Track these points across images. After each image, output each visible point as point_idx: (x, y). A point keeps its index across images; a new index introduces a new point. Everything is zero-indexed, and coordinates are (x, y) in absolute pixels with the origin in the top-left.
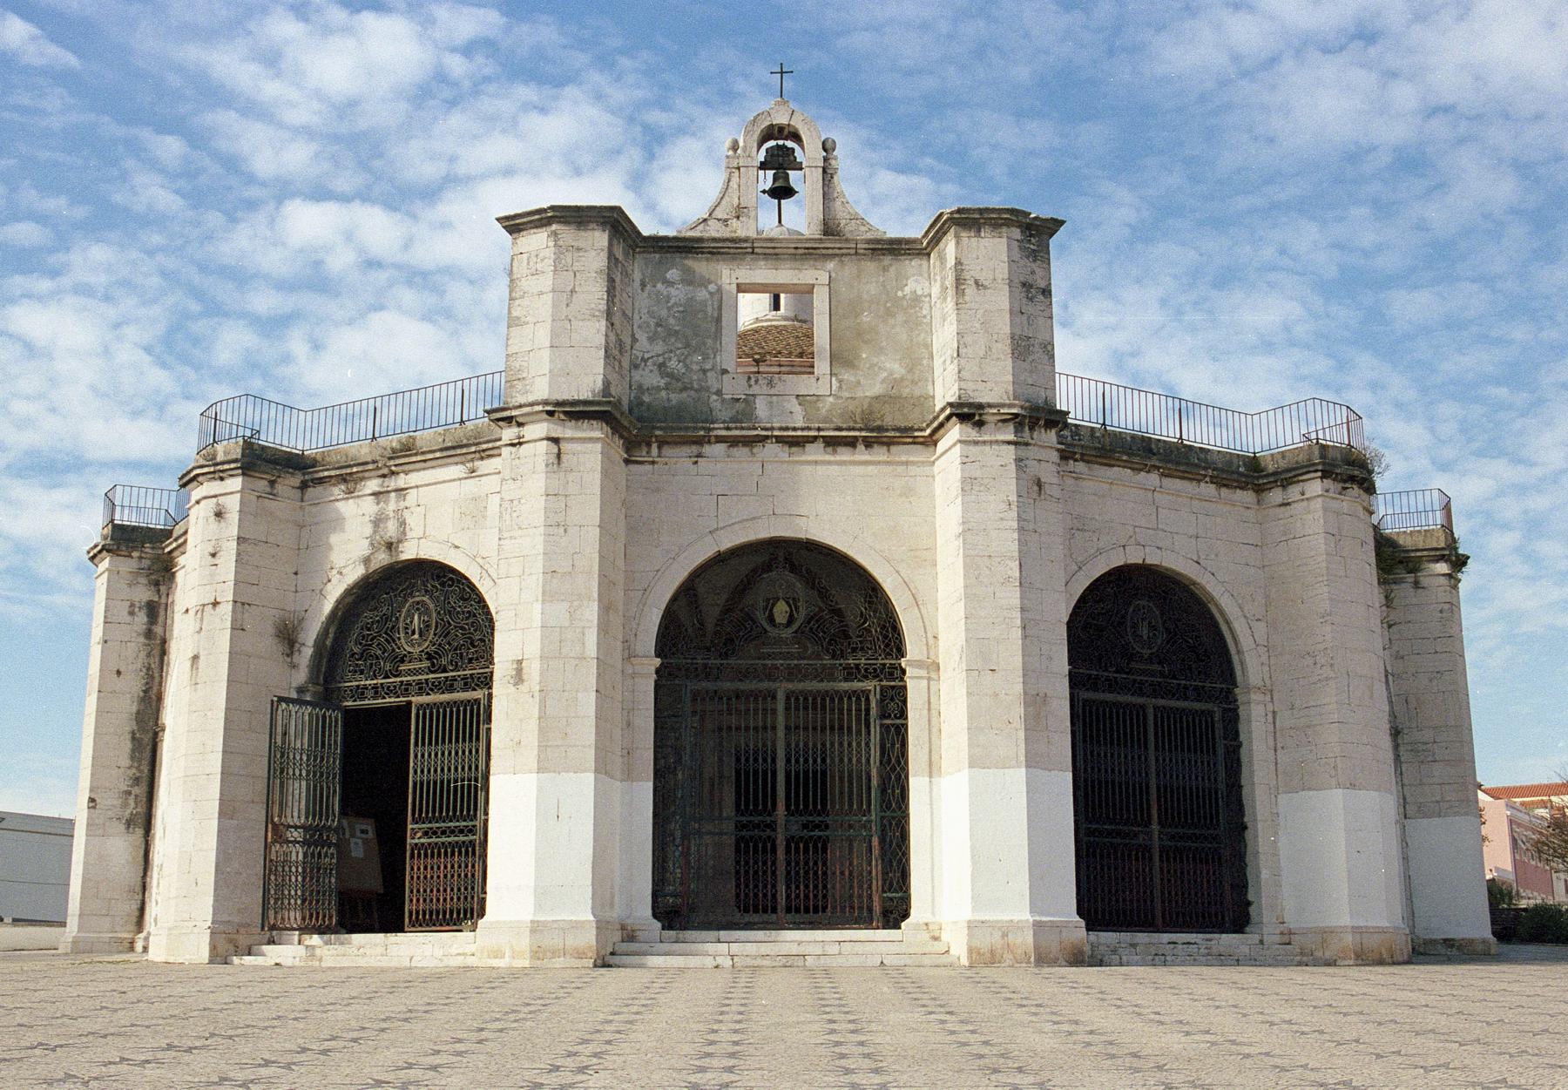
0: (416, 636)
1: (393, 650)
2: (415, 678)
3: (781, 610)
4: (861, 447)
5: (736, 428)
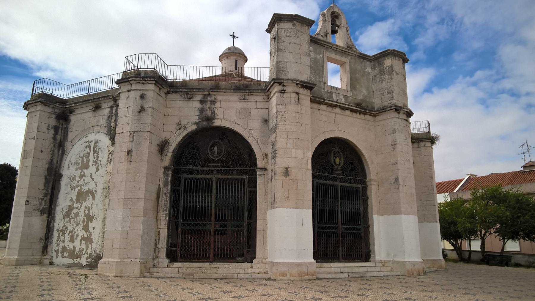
1: (206, 158)
2: (215, 168)
3: (337, 160)
4: (358, 114)
5: (332, 101)
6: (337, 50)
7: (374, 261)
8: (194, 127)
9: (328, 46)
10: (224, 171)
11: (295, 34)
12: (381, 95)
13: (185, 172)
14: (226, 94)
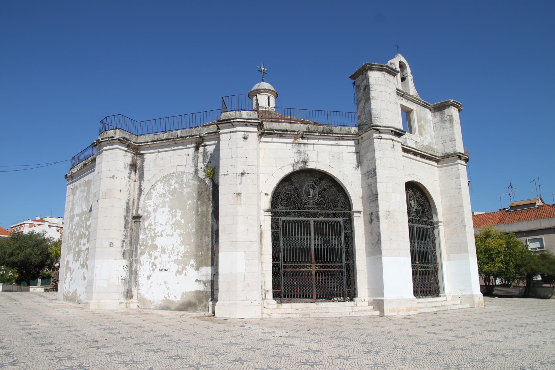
0: (311, 196)
1: (301, 200)
7: (445, 296)
10: (320, 213)
12: (443, 142)
13: (282, 214)
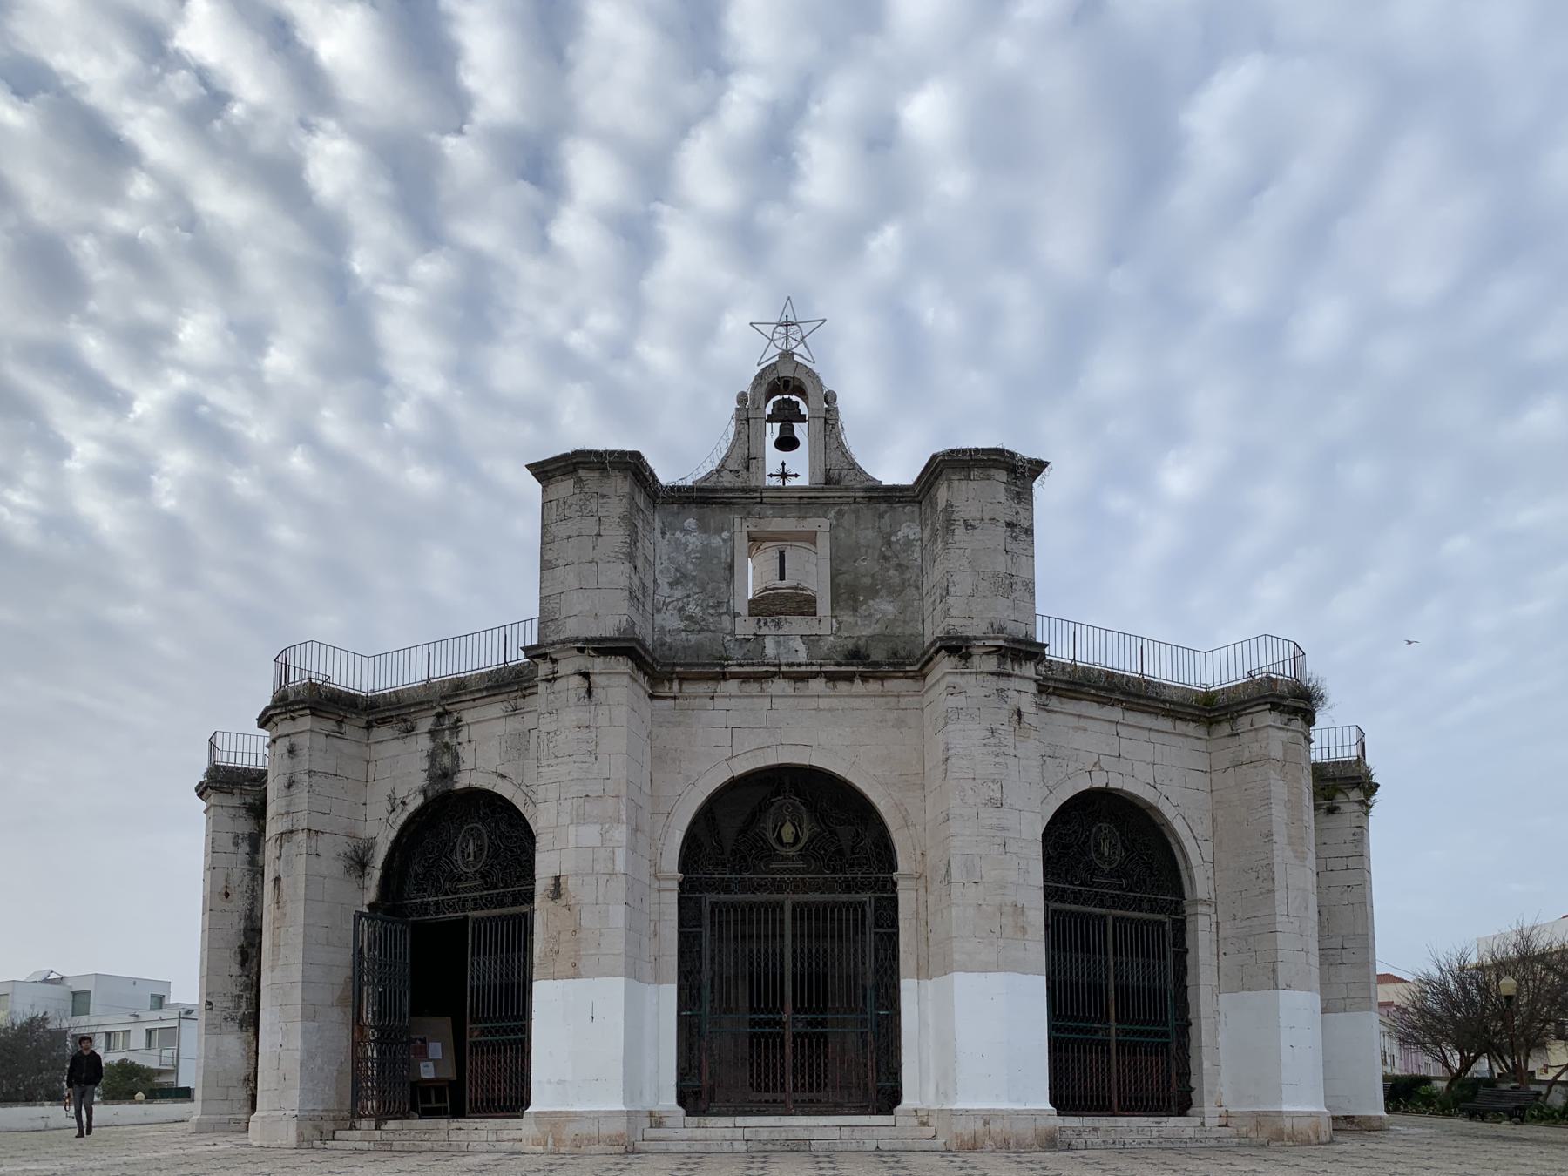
2: (470, 894)
3: (788, 832)
6: (784, 500)
8: (420, 800)
9: (747, 498)
11: (580, 507)
14: (478, 702)
